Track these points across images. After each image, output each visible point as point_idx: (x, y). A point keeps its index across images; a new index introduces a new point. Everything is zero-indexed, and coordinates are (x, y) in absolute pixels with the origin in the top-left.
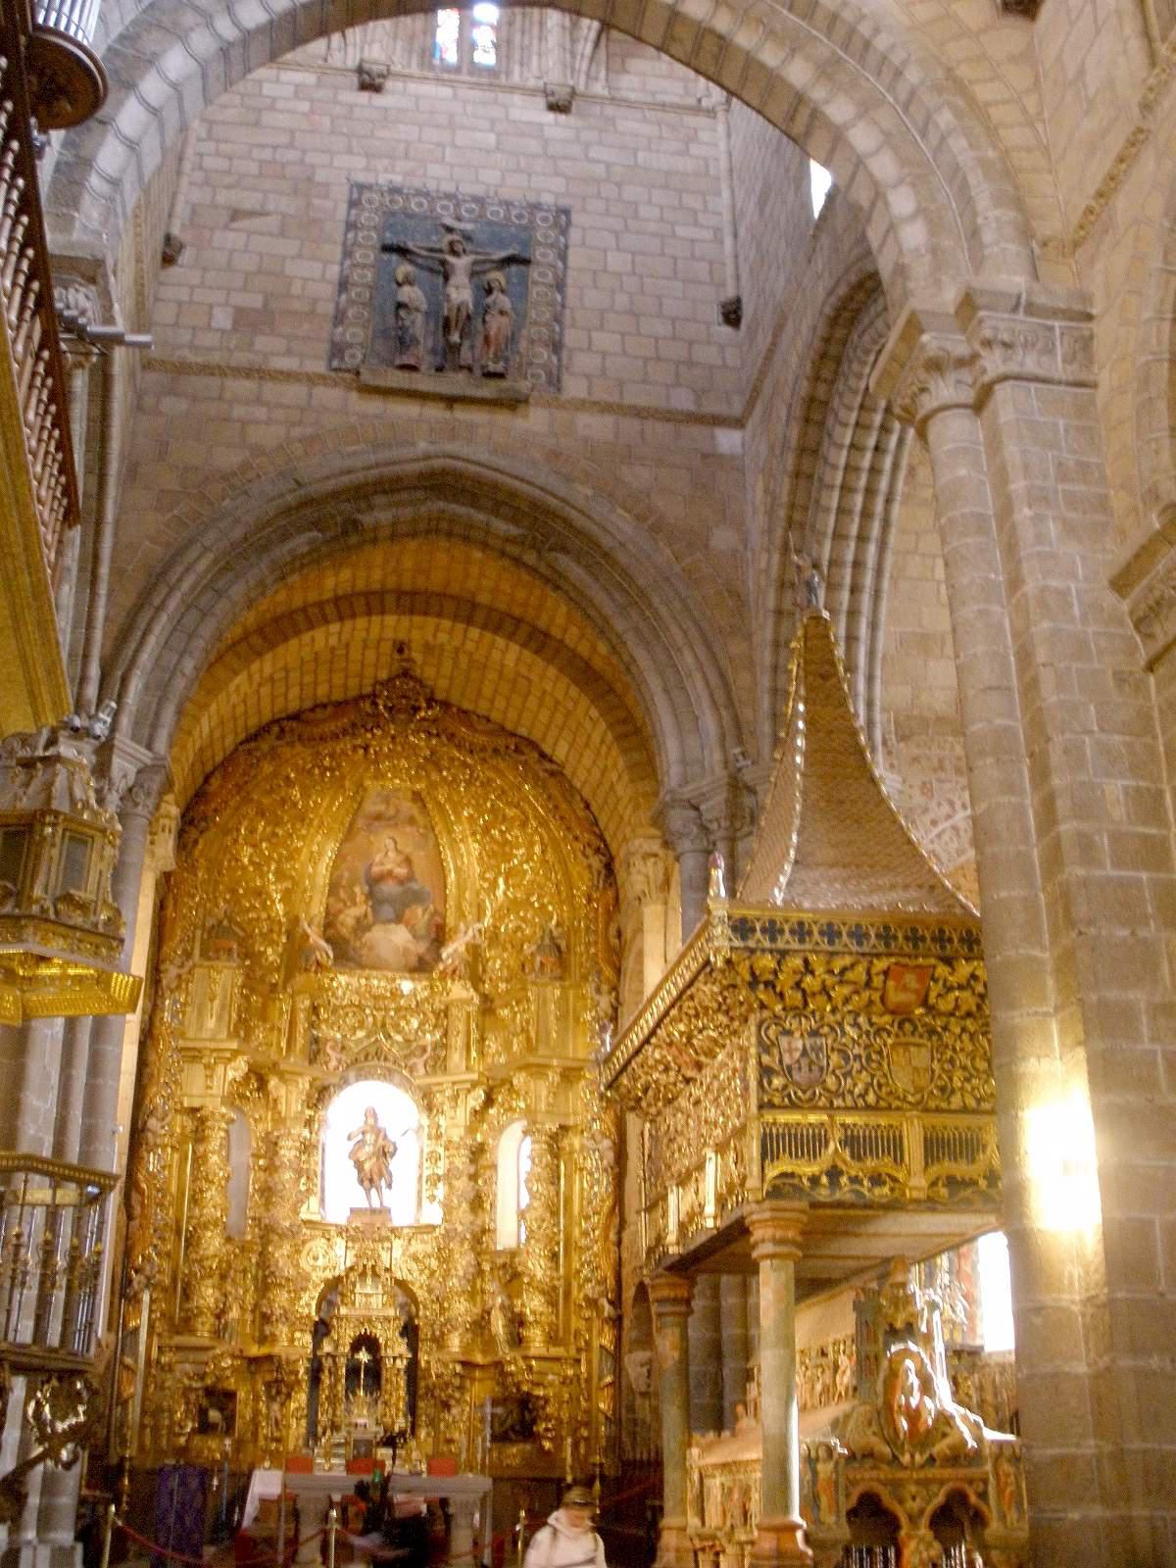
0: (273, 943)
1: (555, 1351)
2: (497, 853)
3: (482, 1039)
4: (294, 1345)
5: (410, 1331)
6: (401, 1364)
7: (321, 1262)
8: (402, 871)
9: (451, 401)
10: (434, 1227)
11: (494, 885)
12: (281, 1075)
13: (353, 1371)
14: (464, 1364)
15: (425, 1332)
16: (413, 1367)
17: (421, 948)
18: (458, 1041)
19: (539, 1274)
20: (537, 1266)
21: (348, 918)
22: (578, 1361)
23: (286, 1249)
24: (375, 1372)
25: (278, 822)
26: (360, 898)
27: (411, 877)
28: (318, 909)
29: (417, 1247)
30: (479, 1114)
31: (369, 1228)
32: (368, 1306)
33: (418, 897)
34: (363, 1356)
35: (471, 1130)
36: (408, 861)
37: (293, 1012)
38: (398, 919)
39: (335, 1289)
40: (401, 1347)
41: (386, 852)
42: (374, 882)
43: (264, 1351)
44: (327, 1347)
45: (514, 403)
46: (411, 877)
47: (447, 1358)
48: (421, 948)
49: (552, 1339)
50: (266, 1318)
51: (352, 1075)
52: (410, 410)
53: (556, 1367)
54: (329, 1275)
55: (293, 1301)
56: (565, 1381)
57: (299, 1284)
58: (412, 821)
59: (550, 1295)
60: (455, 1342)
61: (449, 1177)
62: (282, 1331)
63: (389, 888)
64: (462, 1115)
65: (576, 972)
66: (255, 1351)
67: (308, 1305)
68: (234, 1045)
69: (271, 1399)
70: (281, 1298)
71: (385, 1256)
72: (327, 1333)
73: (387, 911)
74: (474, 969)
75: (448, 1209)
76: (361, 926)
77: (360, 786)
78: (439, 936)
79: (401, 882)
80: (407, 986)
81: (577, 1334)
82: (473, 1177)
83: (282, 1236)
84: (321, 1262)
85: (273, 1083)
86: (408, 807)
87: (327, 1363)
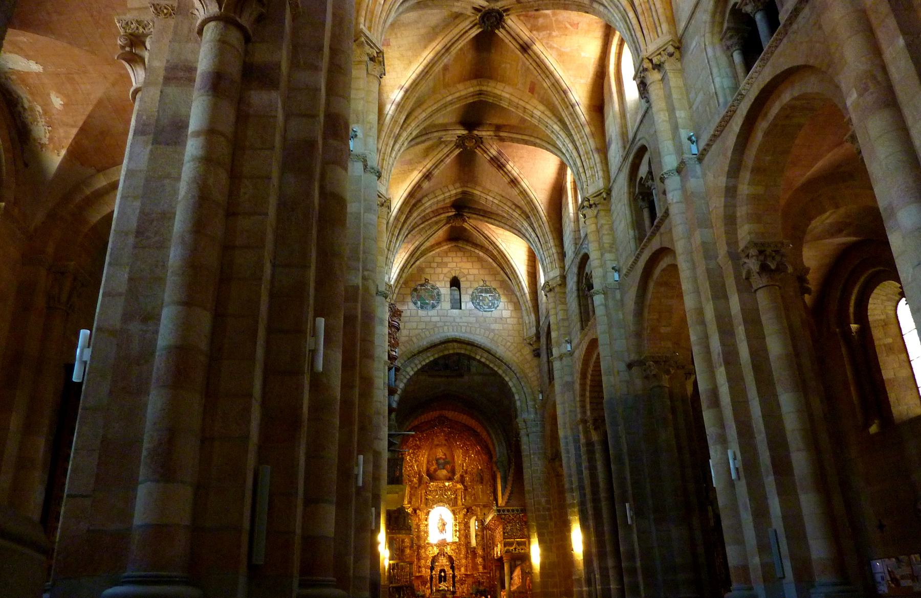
0: (415, 477)
1: (486, 571)
2: (466, 453)
3: (465, 496)
4: (425, 572)
5: (452, 568)
6: (451, 575)
7: (431, 552)
8: (444, 457)
9: (447, 377)
10: (457, 542)
11: (466, 459)
12: (420, 510)
13: (440, 577)
14: (465, 574)
15: (456, 567)
16: (454, 577)
17: (450, 475)
18: (460, 498)
19: (480, 553)
20: (480, 552)
21: (432, 468)
22: (490, 573)
23: (423, 550)
24: (445, 577)
25: (414, 449)
26: (434, 464)
27: (446, 458)
28: (425, 469)
29: (453, 547)
30: (465, 515)
31: (442, 544)
32: (442, 562)
33: (448, 463)
34: (443, 574)
35: (464, 518)
36: (445, 455)
37: (421, 493)
38: (444, 469)
39: (434, 559)
40: (451, 572)
41: (440, 453)
42: (437, 460)
43: (420, 574)
44: (434, 573)
45: (461, 376)
46: (446, 458)
47: (461, 573)
48: (450, 475)
49: (484, 568)
50: (420, 567)
51: (435, 506)
52: (439, 380)
53: (485, 574)
54: (433, 555)
55: (426, 562)
56: (488, 577)
57: (426, 559)
58: (445, 445)
59: (484, 558)
60: (463, 569)
61: (459, 531)
62: (423, 569)
63: (441, 461)
64: (461, 515)
65: (484, 482)
66: (417, 574)
67: (429, 563)
68: (409, 505)
69: (422, 585)
70: (423, 562)
71: (445, 549)
72: (434, 569)
73: (441, 467)
74: (462, 480)
75: (459, 538)
76: (435, 470)
77: (433, 439)
78: (453, 472)
79: (444, 459)
80: (447, 484)
81: (490, 567)
82: (465, 530)
83: (422, 548)
84: (431, 552)
85: (418, 511)
86: (444, 442)
87: (434, 576)
